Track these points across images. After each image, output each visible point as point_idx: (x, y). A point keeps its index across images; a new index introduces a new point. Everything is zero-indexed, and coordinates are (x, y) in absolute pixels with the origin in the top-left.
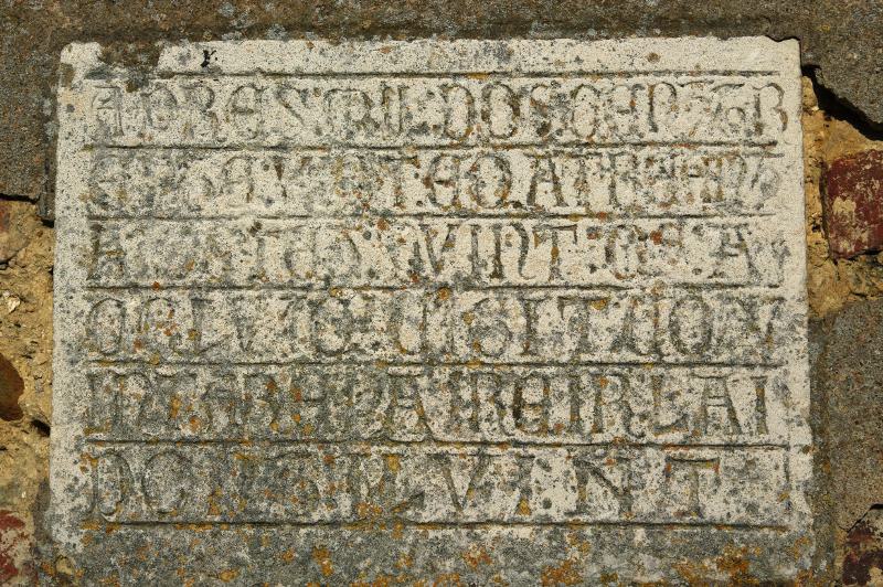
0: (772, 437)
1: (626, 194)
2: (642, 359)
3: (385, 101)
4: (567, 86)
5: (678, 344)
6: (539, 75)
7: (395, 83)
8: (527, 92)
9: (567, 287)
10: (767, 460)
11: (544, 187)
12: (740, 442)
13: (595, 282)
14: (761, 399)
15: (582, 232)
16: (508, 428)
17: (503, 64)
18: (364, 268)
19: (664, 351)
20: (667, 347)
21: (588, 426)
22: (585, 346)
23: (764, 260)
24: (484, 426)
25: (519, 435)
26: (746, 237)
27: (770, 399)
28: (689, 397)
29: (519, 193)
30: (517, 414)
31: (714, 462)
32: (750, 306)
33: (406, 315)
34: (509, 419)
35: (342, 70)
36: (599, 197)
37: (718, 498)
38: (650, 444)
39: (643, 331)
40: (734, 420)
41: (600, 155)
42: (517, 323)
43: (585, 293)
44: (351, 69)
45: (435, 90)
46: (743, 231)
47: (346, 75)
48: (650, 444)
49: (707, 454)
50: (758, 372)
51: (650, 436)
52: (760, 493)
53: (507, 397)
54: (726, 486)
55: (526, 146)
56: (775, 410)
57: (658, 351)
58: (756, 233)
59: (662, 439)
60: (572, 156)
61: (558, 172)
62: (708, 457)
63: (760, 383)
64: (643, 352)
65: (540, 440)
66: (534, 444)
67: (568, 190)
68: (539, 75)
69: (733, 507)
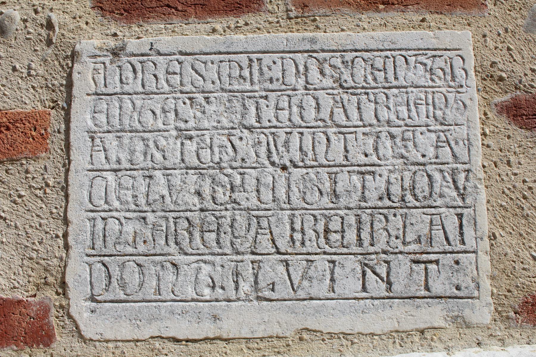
0: (467, 247)
1: (384, 114)
2: (395, 205)
3: (250, 66)
4: (349, 56)
5: (415, 196)
6: (333, 51)
7: (254, 56)
8: (326, 60)
9: (352, 165)
10: (465, 260)
11: (339, 111)
12: (451, 250)
13: (367, 163)
14: (461, 226)
15: (360, 136)
16: (321, 245)
17: (313, 46)
18: (239, 158)
19: (407, 200)
20: (409, 197)
21: (366, 243)
22: (364, 198)
23: (461, 151)
24: (308, 243)
25: (328, 249)
26: (449, 136)
27: (465, 225)
28: (422, 226)
29: (325, 114)
30: (326, 238)
31: (437, 262)
32: (454, 173)
33: (263, 183)
34: (322, 240)
35: (225, 50)
36: (369, 117)
37: (439, 282)
38: (401, 253)
39: (396, 190)
40: (447, 239)
41: (367, 94)
42: (327, 186)
43: (363, 169)
44: (230, 50)
45: (276, 60)
46: (447, 134)
47: (228, 53)
48: (401, 253)
49: (432, 257)
50: (459, 211)
51: (401, 248)
52: (462, 278)
53: (321, 227)
54: (443, 275)
55: (326, 89)
56: (469, 232)
57: (403, 200)
58: (454, 134)
59: (407, 249)
60: (352, 94)
61: (346, 103)
62: (433, 259)
63: (460, 216)
64: (395, 201)
65: (339, 251)
66: (335, 254)
67: (354, 114)
68: (333, 51)
69: (447, 287)
